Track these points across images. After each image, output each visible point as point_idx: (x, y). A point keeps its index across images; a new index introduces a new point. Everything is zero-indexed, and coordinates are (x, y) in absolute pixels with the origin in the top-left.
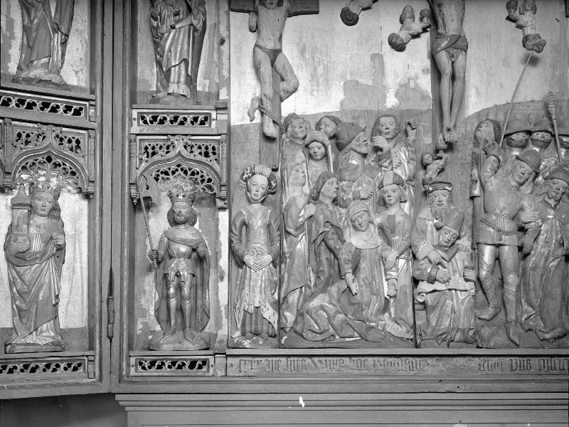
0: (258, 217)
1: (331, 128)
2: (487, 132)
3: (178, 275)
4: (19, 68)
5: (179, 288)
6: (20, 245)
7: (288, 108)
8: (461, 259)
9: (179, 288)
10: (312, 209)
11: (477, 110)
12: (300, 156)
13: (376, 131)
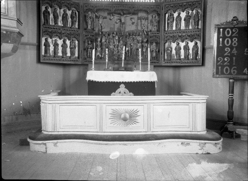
0: (99, 43)
1: (108, 33)
2: (127, 34)
3: (89, 51)
4: (71, 26)
5: (89, 52)
6: (71, 47)
7: (103, 30)
9: (89, 52)
10: (105, 43)
11: (127, 31)
12: (104, 37)
13: (113, 33)
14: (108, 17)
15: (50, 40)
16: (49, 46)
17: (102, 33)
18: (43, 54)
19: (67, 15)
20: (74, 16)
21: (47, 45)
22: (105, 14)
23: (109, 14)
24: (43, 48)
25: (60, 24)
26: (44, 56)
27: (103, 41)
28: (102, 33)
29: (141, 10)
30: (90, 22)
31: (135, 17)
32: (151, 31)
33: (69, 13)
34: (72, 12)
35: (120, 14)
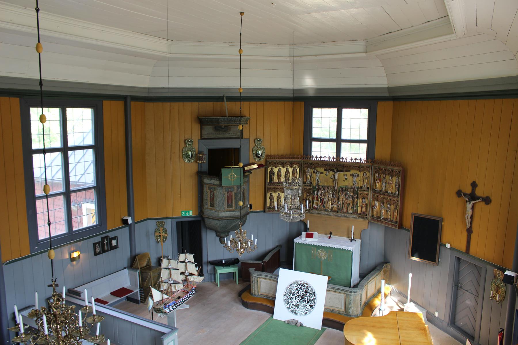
0: (315, 196)
8: (336, 203)
14: (325, 172)
15: (274, 194)
16: (273, 199)
17: (319, 186)
18: (268, 205)
19: (289, 172)
20: (295, 172)
21: (271, 198)
22: (322, 170)
23: (325, 170)
24: (268, 200)
25: (283, 179)
26: (269, 208)
27: (319, 194)
28: (319, 186)
29: (353, 169)
30: (309, 177)
31: (348, 174)
32: (361, 187)
33: (290, 170)
34: (293, 170)
35: (333, 171)
